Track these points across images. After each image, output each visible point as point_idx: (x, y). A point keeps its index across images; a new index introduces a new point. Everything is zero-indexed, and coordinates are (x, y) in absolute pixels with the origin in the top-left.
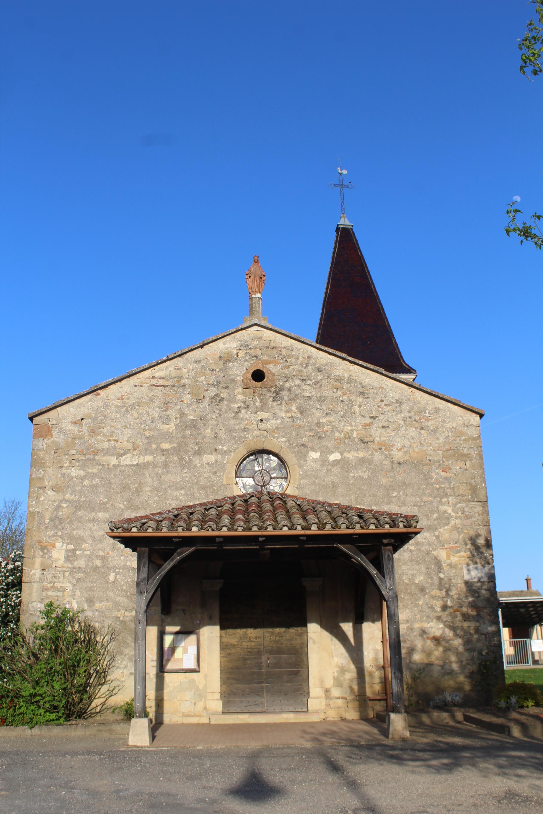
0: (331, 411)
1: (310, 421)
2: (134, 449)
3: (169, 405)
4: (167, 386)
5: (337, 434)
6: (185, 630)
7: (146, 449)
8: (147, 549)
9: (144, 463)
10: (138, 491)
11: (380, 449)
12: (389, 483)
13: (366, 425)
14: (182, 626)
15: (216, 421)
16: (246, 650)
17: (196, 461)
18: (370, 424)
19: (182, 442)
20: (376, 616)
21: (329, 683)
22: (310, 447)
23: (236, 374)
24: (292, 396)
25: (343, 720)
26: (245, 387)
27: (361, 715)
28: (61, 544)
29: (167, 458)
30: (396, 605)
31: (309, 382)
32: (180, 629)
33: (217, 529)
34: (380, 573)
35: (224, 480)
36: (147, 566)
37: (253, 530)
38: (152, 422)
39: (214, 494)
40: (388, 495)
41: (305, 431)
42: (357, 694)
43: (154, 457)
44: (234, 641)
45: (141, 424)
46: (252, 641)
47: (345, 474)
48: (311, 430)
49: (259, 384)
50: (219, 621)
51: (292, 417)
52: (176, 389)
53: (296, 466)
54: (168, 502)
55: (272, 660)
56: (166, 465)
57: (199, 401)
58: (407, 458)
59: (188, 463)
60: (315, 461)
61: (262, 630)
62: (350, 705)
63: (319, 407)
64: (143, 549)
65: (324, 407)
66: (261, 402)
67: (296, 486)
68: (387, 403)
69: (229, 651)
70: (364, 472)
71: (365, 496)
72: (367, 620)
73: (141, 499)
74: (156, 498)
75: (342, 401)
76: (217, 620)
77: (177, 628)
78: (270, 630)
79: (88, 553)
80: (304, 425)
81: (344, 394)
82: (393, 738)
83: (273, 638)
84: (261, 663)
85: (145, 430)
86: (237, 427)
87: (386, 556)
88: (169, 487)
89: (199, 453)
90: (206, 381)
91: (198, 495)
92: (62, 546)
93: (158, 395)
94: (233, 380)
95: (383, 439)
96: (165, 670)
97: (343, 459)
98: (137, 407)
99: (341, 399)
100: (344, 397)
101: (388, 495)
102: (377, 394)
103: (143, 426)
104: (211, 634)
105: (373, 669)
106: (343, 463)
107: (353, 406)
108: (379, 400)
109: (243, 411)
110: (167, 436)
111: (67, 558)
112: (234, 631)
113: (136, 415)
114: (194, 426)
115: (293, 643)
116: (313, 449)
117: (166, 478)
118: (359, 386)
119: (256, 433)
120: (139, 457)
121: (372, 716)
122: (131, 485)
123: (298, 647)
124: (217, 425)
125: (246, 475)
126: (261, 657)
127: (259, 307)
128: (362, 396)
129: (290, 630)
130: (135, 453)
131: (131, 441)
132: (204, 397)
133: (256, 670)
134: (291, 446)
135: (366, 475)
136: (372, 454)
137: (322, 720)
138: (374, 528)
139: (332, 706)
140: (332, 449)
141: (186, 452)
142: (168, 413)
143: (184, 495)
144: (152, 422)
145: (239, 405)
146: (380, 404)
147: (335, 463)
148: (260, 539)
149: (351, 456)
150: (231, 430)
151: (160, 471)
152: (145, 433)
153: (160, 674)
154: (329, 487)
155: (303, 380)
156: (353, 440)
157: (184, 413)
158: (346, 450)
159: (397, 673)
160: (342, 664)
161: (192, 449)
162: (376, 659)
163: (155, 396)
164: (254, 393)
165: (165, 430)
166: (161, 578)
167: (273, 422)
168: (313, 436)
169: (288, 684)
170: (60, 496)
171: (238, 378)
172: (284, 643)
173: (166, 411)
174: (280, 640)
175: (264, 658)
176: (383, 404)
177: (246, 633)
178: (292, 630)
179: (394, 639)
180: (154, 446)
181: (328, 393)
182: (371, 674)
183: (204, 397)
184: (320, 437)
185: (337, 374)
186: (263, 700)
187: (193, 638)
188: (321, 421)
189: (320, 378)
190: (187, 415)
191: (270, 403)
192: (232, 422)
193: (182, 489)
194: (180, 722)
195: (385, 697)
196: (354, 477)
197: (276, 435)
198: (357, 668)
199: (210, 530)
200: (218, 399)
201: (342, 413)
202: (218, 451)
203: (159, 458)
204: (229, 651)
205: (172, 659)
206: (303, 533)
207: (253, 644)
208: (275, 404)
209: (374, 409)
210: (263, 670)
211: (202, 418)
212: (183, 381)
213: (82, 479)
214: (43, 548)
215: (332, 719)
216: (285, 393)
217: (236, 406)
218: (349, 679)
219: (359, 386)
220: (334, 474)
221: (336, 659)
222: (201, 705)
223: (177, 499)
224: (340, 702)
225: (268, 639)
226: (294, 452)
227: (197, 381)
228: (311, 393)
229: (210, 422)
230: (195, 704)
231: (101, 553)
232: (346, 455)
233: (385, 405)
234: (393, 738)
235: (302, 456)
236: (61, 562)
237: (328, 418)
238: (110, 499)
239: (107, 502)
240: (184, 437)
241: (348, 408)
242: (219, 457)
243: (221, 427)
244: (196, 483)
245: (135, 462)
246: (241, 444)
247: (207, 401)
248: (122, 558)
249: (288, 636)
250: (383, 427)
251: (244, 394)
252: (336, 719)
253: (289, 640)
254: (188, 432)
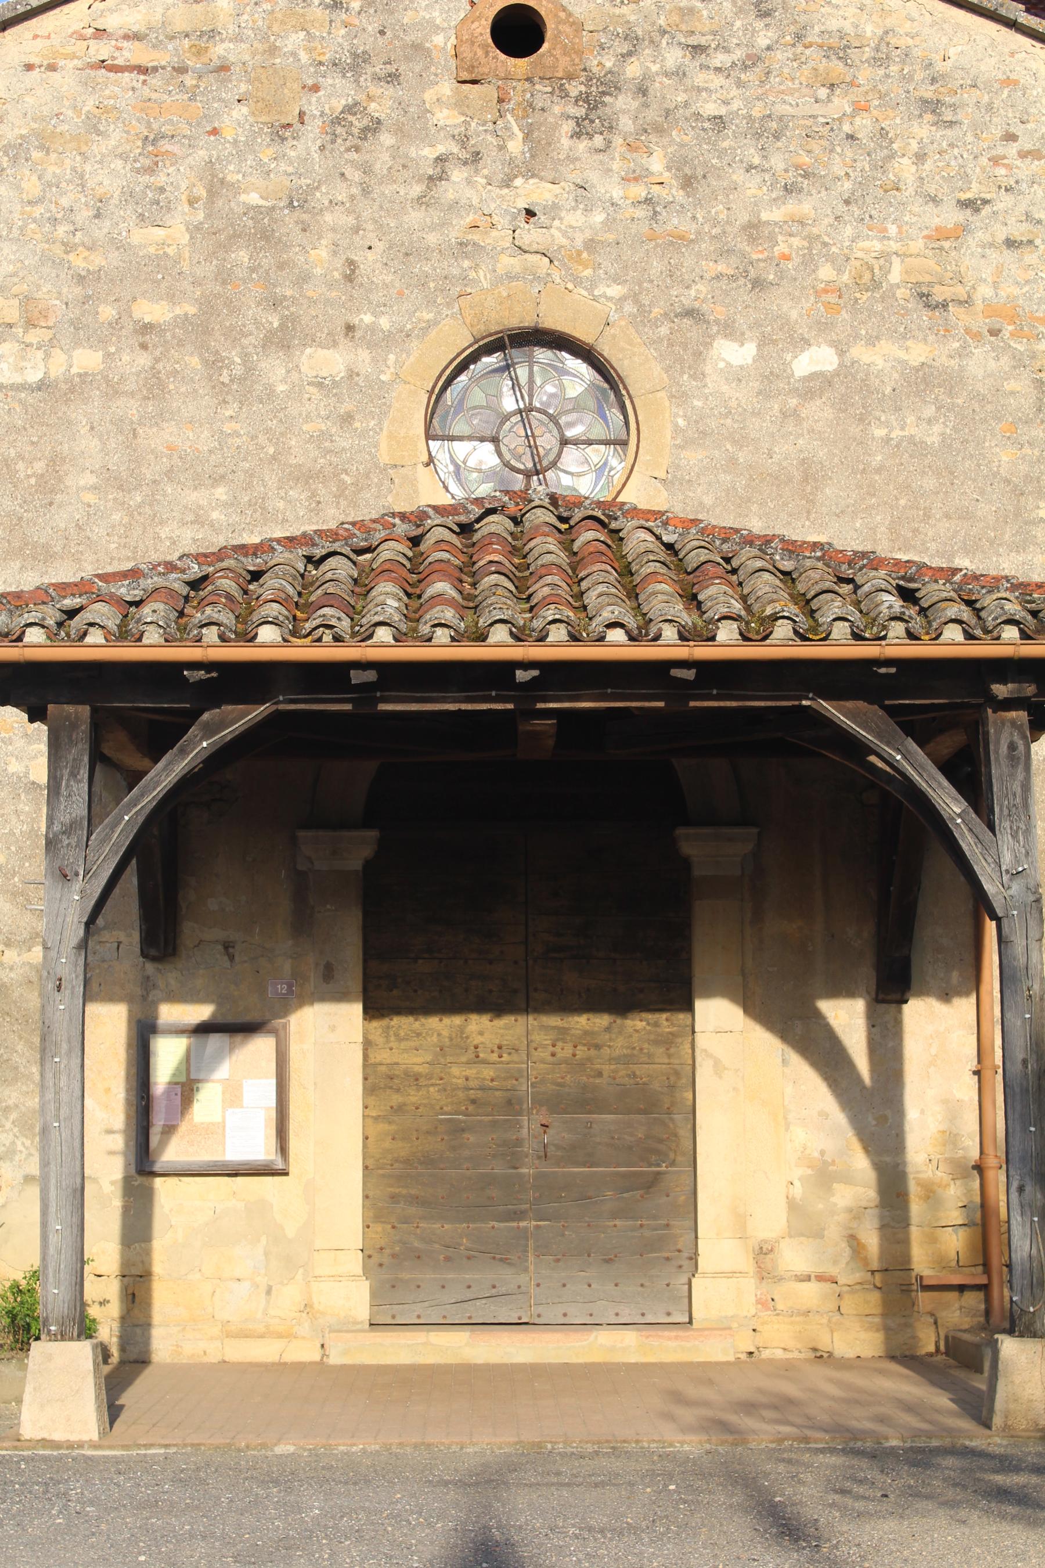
0: (806, 175)
1: (722, 216)
2: (30, 324)
3: (165, 145)
4: (155, 69)
6: (230, 1019)
7: (76, 325)
8: (85, 710)
9: (68, 380)
10: (49, 487)
11: (994, 332)
12: (1023, 468)
13: (940, 235)
14: (220, 1001)
15: (349, 212)
16: (461, 1094)
17: (274, 370)
18: (961, 231)
19: (218, 296)
20: (955, 975)
21: (770, 1221)
22: (717, 322)
23: (431, 22)
24: (652, 115)
25: (821, 1357)
26: (465, 76)
27: (888, 1340)
29: (157, 360)
30: (1034, 934)
31: (720, 59)
32: (214, 1015)
33: (354, 634)
34: (977, 812)
35: (383, 446)
36: (84, 773)
37: (491, 640)
38: (97, 216)
39: (343, 503)
40: (1017, 514)
41: (699, 255)
42: (875, 1265)
43: (108, 355)
44: (417, 1061)
45: (54, 221)
46: (485, 1062)
47: (855, 430)
48: (726, 253)
49: (520, 65)
50: (359, 987)
51: (648, 201)
52: (189, 80)
53: (662, 394)
54: (164, 532)
55: (558, 1134)
56: (154, 386)
57: (282, 132)
59: (242, 380)
60: (737, 376)
61: (522, 1019)
62: (848, 1305)
63: (756, 161)
64: (70, 709)
65: (777, 162)
66: (527, 137)
67: (662, 475)
68: (1028, 147)
69: (396, 1099)
70: (929, 422)
71: (927, 516)
72: (922, 993)
73: (61, 518)
74: (116, 517)
75: (851, 137)
76: (355, 983)
77: (202, 1012)
78: (554, 1021)
80: (698, 233)
81: (860, 108)
82: (1006, 1427)
83: (565, 1051)
84: (519, 1142)
85: (69, 248)
86: (432, 239)
87: (1004, 749)
88: (170, 474)
89: (284, 339)
90: (310, 50)
91: (281, 505)
93: (121, 104)
94: (418, 48)
95: (1008, 290)
96: (157, 1168)
97: (847, 370)
98: (36, 155)
99: (847, 128)
100: (858, 121)
101: (1017, 514)
102: (990, 107)
103: (62, 230)
104: (330, 1033)
105: (941, 1175)
106: (846, 388)
107: (891, 157)
108: (998, 133)
109: (457, 175)
110: (157, 272)
112: (417, 1025)
113: (32, 186)
114: (263, 232)
115: (641, 1070)
116: (729, 330)
117: (157, 438)
118: (919, 76)
119: (509, 262)
120: (47, 356)
121: (931, 1348)
122: (21, 465)
123: (656, 1086)
124: (356, 230)
125: (466, 431)
126: (518, 1122)
128: (929, 117)
129: (629, 1022)
130: (33, 337)
131: (15, 290)
132: (301, 114)
133: (499, 1169)
134: (642, 317)
135: (933, 436)
136: (962, 353)
137: (743, 1357)
138: (960, 637)
139: (780, 1306)
140: (803, 331)
141: (234, 335)
142: (161, 179)
143: (225, 505)
144: (97, 216)
145: (441, 149)
146: (1000, 151)
147: (817, 385)
148: (521, 676)
149: (879, 358)
150: (409, 253)
151: (131, 408)
152: (72, 257)
153: (140, 1180)
154: (790, 480)
155: (698, 49)
156: (889, 296)
157: (222, 181)
158: (857, 337)
159: (1028, 1189)
160: (822, 1153)
161: (256, 322)
162: (950, 1138)
163: (107, 110)
164: (500, 101)
165: (152, 250)
166: (141, 819)
167: (575, 218)
168: (733, 278)
169: (618, 1222)
171: (439, 39)
172: (607, 1069)
173: (150, 170)
174: (589, 1059)
175: (528, 1126)
176: (1013, 149)
177: (461, 1030)
178: (637, 1024)
179: (1025, 1062)
180: (107, 312)
181: (795, 103)
182: (930, 1193)
183: (301, 114)
184: (758, 284)
185: (833, 24)
186: (523, 1279)
187: (260, 1049)
188: (765, 216)
189: (763, 42)
190: (235, 189)
191: (566, 142)
192: (415, 217)
193: (217, 480)
194: (213, 1358)
195: (983, 1280)
196: (887, 440)
197: (588, 272)
198: (879, 1167)
199: (328, 638)
200: (358, 123)
201: (848, 185)
202: (358, 334)
203: (126, 358)
204: (396, 1099)
205: (183, 1128)
206: (682, 652)
207: (488, 1072)
208: (583, 145)
209: (975, 173)
210: (524, 1170)
211: (297, 202)
212: (219, 50)
215: (779, 1354)
216: (623, 103)
217: (430, 153)
218: (850, 1210)
219: (919, 76)
220: (812, 431)
221: (800, 1135)
222: (289, 1296)
224: (811, 1293)
225: (545, 1054)
226: (656, 342)
227: (273, 50)
228: (726, 103)
229: (328, 218)
230: (269, 1292)
232: (860, 353)
233: (1023, 155)
234: (1006, 1427)
235: (688, 358)
237: (791, 207)
240: (224, 277)
241: (874, 167)
242: (364, 355)
243: (371, 238)
244: (274, 458)
245: (34, 376)
246: (448, 305)
247: (312, 133)
249: (619, 1046)
250: (1011, 243)
251: (460, 104)
252: (795, 1355)
253: (627, 1060)
254: (242, 256)
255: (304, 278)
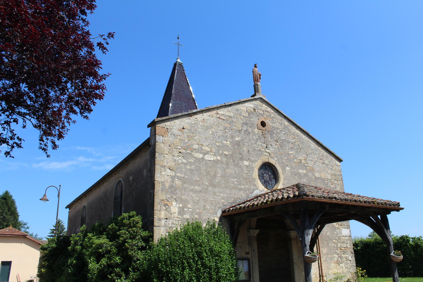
5: (295, 160)
10: (215, 176)
17: (241, 163)
24: (277, 138)
28: (175, 203)
31: (283, 133)
43: (221, 158)
49: (264, 128)
58: (319, 176)
79: (191, 210)
89: (242, 159)
92: (176, 205)
110: (225, 147)
111: (179, 213)
114: (238, 143)
116: (287, 166)
117: (229, 171)
124: (249, 146)
127: (260, 89)
151: (224, 166)
155: (281, 131)
170: (173, 174)
180: (221, 152)
192: (255, 145)
193: (236, 178)
213: (185, 164)
214: (166, 205)
223: (233, 183)
231: (198, 211)
232: (299, 171)
235: (284, 169)
236: (176, 215)
238: (200, 178)
239: (199, 180)
245: (212, 159)
248: (209, 214)
255: (243, 151)
